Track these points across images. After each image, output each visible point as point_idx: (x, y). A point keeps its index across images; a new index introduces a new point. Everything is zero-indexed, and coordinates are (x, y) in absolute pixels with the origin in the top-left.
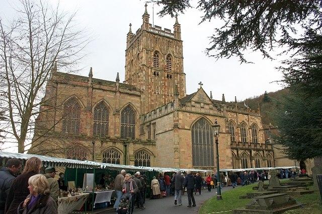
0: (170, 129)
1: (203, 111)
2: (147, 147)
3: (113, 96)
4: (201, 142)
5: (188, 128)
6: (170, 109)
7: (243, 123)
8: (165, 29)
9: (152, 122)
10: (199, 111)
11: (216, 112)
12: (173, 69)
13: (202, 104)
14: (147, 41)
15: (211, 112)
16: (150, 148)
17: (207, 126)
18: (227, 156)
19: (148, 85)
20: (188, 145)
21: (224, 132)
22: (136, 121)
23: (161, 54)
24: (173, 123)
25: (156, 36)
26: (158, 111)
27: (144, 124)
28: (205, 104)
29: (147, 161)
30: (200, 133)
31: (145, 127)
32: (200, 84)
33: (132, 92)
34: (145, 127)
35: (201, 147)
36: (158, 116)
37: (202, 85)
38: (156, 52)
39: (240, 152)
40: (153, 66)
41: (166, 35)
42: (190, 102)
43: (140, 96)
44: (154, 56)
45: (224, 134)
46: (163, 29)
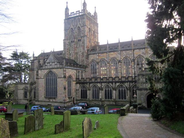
1: (51, 67)
8: (76, 12)
10: (49, 67)
15: (56, 66)
20: (43, 86)
30: (51, 79)
35: (50, 87)
38: (72, 29)
46: (75, 13)
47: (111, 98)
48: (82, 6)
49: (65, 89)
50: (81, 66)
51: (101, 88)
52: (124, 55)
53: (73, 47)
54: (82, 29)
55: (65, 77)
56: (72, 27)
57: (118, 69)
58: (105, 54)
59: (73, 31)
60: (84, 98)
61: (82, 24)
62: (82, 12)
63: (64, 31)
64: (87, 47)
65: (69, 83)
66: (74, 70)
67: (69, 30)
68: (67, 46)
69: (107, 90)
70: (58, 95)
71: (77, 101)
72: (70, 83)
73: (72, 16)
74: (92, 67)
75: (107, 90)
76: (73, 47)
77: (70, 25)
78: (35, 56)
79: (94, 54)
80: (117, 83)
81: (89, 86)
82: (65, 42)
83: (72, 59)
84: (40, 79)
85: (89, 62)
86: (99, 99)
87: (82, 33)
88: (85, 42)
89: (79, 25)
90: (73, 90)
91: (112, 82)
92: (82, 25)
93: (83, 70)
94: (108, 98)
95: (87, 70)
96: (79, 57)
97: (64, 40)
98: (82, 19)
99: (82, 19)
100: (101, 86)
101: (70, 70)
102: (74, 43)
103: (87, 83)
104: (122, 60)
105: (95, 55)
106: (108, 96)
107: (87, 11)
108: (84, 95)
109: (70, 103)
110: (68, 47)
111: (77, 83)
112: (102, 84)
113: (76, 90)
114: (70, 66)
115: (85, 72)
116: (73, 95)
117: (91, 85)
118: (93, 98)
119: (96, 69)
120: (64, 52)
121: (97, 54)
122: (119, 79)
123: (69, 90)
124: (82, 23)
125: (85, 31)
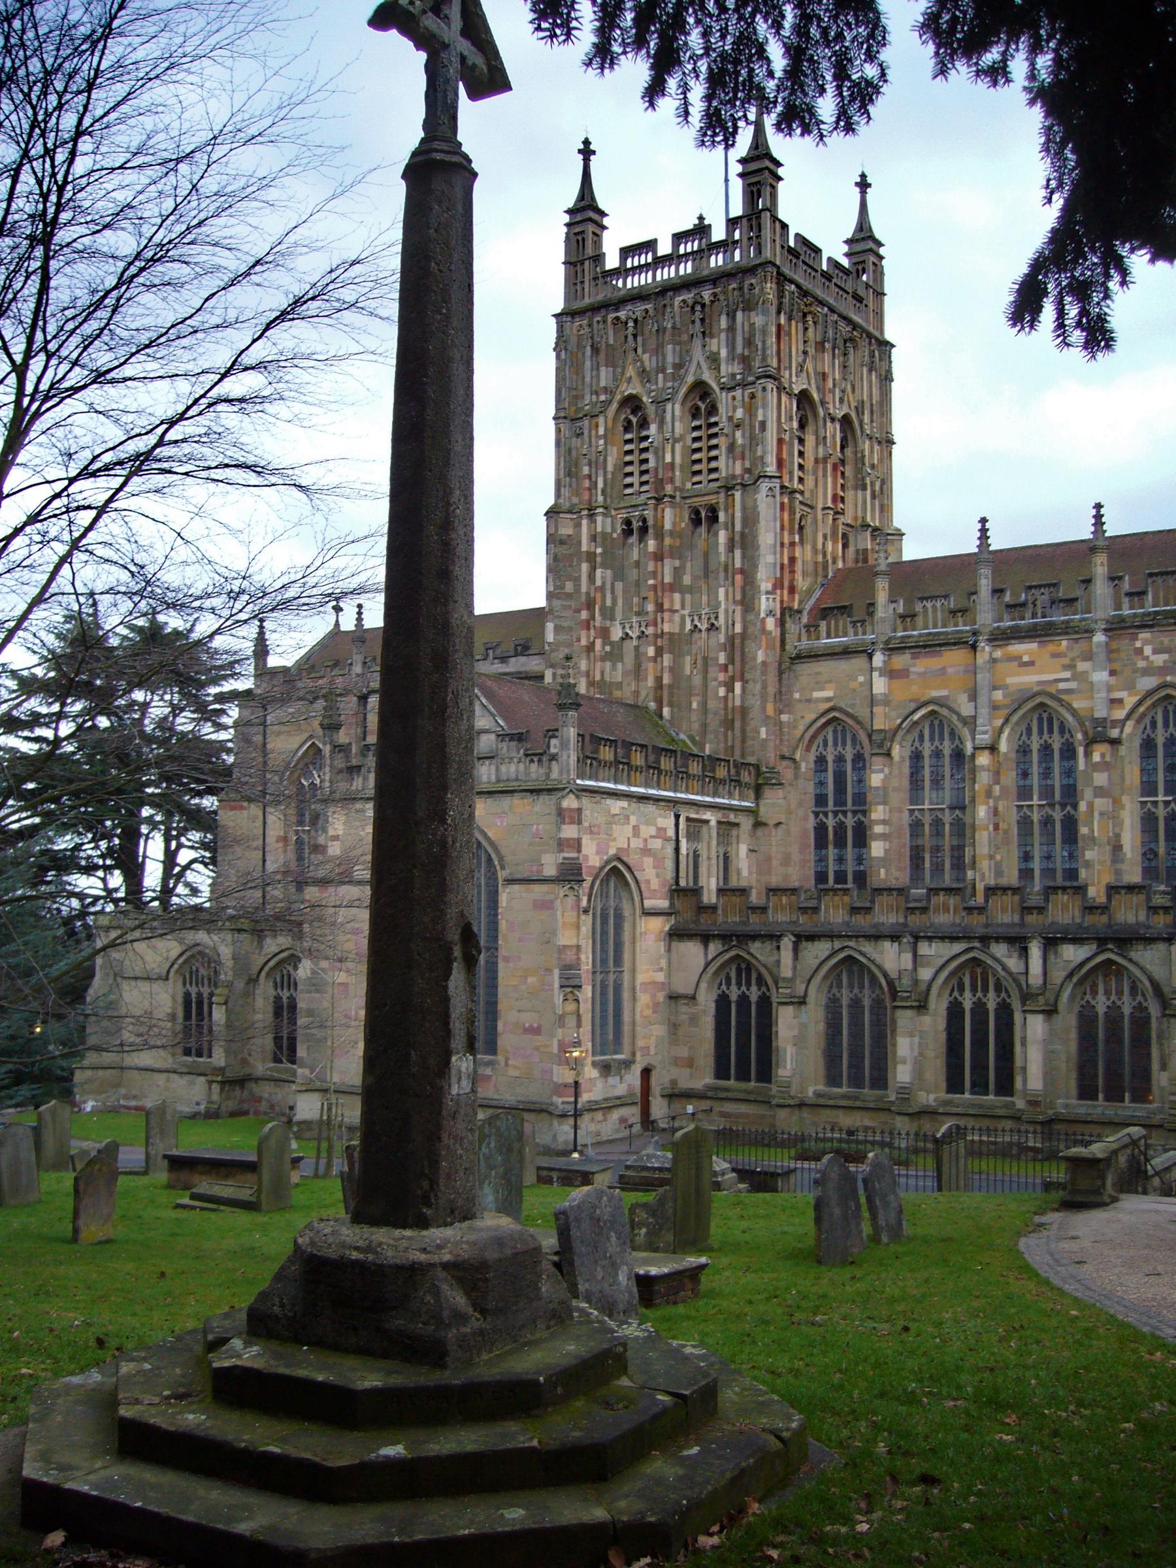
8: (679, 238)
25: (622, 314)
38: (632, 403)
46: (664, 248)
47: (1006, 1086)
48: (737, 186)
49: (571, 985)
50: (721, 772)
51: (906, 982)
52: (1146, 672)
53: (638, 584)
54: (729, 407)
55: (570, 874)
57: (1083, 806)
58: (954, 659)
59: (644, 424)
60: (743, 1076)
61: (732, 357)
62: (725, 246)
63: (550, 427)
64: (778, 584)
65: (604, 933)
66: (650, 808)
67: (601, 420)
68: (585, 567)
69: (968, 1005)
70: (506, 1040)
71: (677, 1106)
72: (618, 928)
73: (633, 282)
74: (821, 784)
75: (968, 1005)
76: (638, 584)
77: (611, 363)
78: (273, 661)
79: (846, 652)
80: (1065, 940)
81: (795, 968)
82: (566, 530)
83: (626, 694)
85: (798, 733)
86: (885, 1087)
87: (731, 448)
88: (767, 537)
89: (698, 369)
90: (644, 999)
91: (1019, 943)
92: (737, 368)
93: (731, 808)
94: (980, 1086)
95: (773, 803)
96: (697, 681)
97: (551, 514)
98: (732, 316)
99: (732, 316)
100: (910, 966)
101: (617, 806)
102: (651, 545)
103: (774, 937)
104: (1120, 714)
105: (859, 662)
106: (979, 1067)
107: (784, 226)
108: (743, 1048)
109: (616, 1115)
110: (591, 578)
111: (676, 935)
112: (924, 949)
113: (673, 997)
114: (622, 767)
115: (758, 824)
116: (640, 1043)
117: (817, 951)
118: (833, 1079)
119: (861, 799)
120: (550, 626)
121: (878, 659)
122: (1090, 909)
123: (604, 987)
124: (731, 346)
125: (763, 424)
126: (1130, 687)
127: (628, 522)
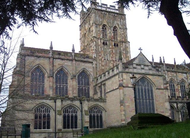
0: (117, 88)
2: (100, 104)
3: (70, 64)
4: (142, 97)
5: (131, 86)
6: (116, 72)
7: (183, 81)
8: (111, 6)
9: (103, 83)
10: (140, 71)
11: (154, 72)
12: (119, 39)
13: (142, 66)
14: (96, 17)
15: (151, 72)
16: (101, 104)
17: (148, 83)
18: (166, 109)
19: (97, 52)
20: (132, 100)
21: (163, 88)
22: (90, 84)
23: (108, 27)
24: (118, 83)
25: (103, 13)
26: (107, 73)
27: (96, 85)
28: (145, 65)
29: (99, 115)
31: (97, 88)
32: (140, 49)
33: (86, 60)
34: (97, 88)
35: (143, 102)
36: (107, 78)
37: (142, 50)
38: (104, 26)
39: (179, 105)
40: (102, 38)
41: (112, 11)
42: (132, 64)
43: (92, 63)
44: (103, 28)
45: (162, 90)
46: (109, 6)
56: (106, 24)
84: (127, 88)
98: (120, 20)
126: (169, 78)
127: (104, 42)
